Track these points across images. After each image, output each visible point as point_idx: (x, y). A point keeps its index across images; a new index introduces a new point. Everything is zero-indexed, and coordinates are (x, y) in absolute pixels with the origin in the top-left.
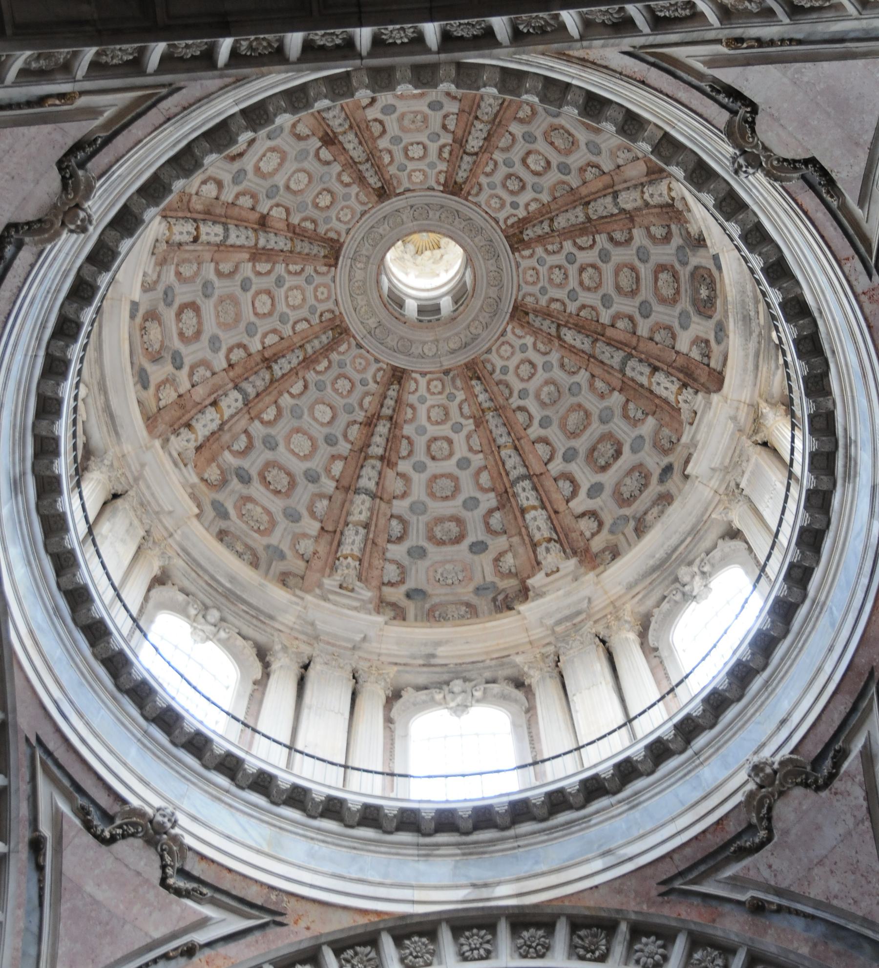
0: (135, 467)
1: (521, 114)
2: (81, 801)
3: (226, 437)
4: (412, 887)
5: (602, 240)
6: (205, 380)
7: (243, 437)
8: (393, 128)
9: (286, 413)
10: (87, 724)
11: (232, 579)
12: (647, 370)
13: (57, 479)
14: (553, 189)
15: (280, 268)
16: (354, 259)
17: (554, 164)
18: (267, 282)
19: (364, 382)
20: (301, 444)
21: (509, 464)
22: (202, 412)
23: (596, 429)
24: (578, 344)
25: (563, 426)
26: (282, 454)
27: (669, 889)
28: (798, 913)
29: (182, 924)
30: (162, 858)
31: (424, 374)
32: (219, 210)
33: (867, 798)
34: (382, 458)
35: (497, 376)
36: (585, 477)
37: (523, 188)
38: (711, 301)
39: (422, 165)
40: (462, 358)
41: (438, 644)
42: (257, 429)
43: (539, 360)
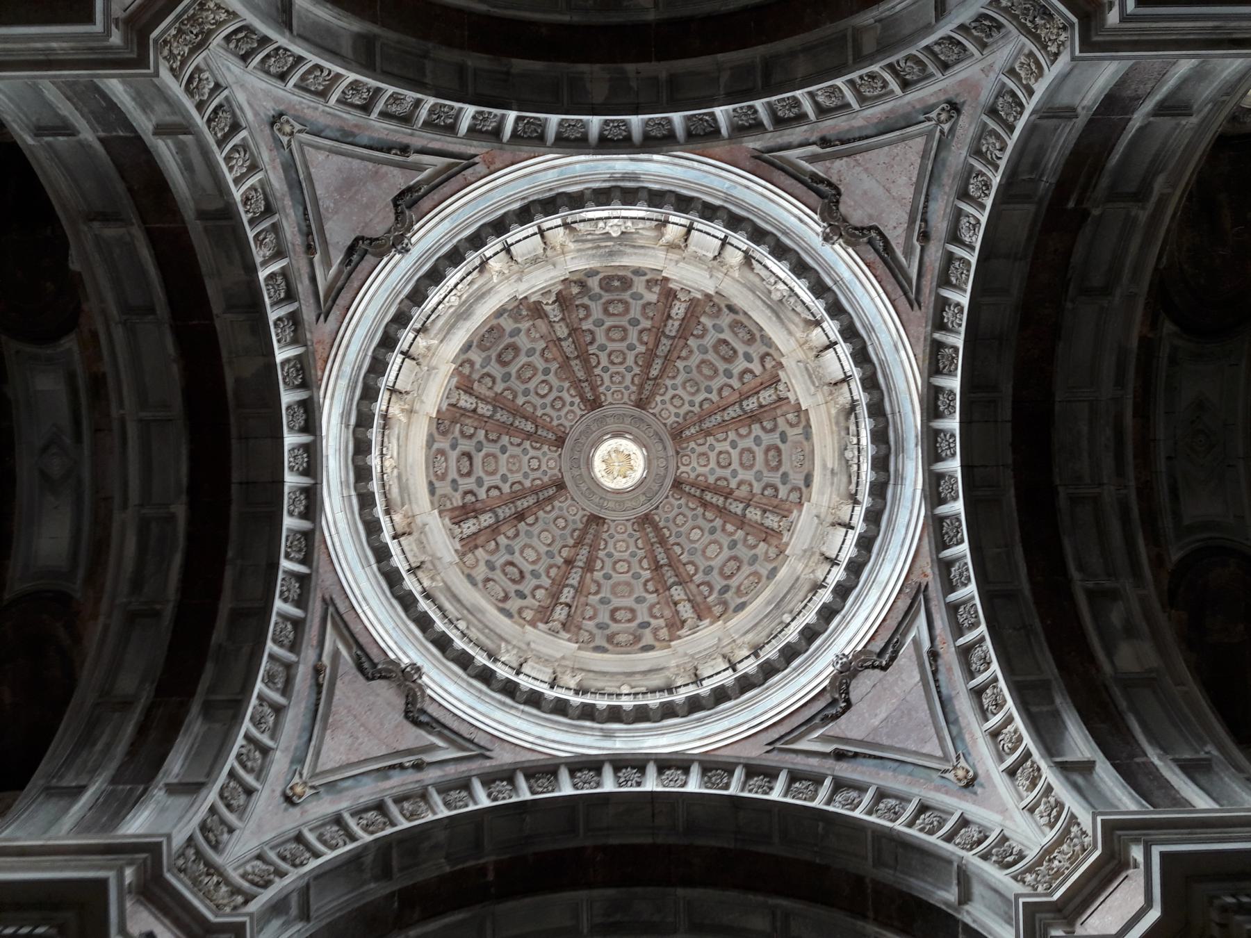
0: (686, 659)
1: (510, 397)
2: (817, 721)
3: (699, 599)
4: (915, 490)
5: (592, 349)
6: (660, 609)
8: (518, 477)
9: (692, 558)
10: (771, 709)
11: (769, 603)
12: (670, 322)
13: (611, 708)
14: (561, 379)
16: (602, 507)
17: (544, 378)
19: (680, 507)
20: (712, 550)
21: (733, 414)
22: (677, 612)
23: (711, 356)
24: (658, 367)
25: (711, 378)
26: (716, 563)
28: (925, 207)
29: (914, 658)
30: (867, 667)
31: (678, 468)
32: (554, 589)
33: (841, 157)
34: (726, 498)
35: (680, 420)
36: (740, 365)
37: (560, 398)
38: (621, 278)
39: (544, 460)
40: (669, 443)
41: (824, 466)
42: (698, 578)
43: (671, 392)
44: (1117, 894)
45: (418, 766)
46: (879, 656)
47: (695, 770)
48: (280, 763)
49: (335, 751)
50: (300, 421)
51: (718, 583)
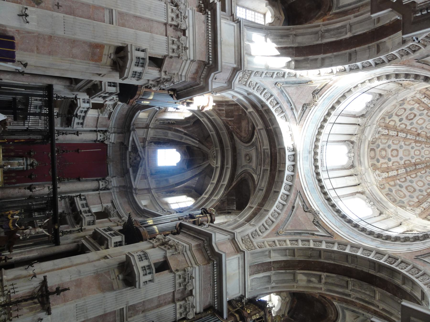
2: (303, 203)
3: (398, 177)
6: (396, 165)
7: (404, 179)
11: (381, 199)
15: (423, 146)
18: (420, 148)
26: (414, 184)
27: (417, 258)
42: (409, 178)
44: (233, 249)
45: (292, 109)
46: (317, 223)
47: (293, 173)
48: (283, 80)
49: (291, 90)
50: (378, 62)
51: (405, 185)
